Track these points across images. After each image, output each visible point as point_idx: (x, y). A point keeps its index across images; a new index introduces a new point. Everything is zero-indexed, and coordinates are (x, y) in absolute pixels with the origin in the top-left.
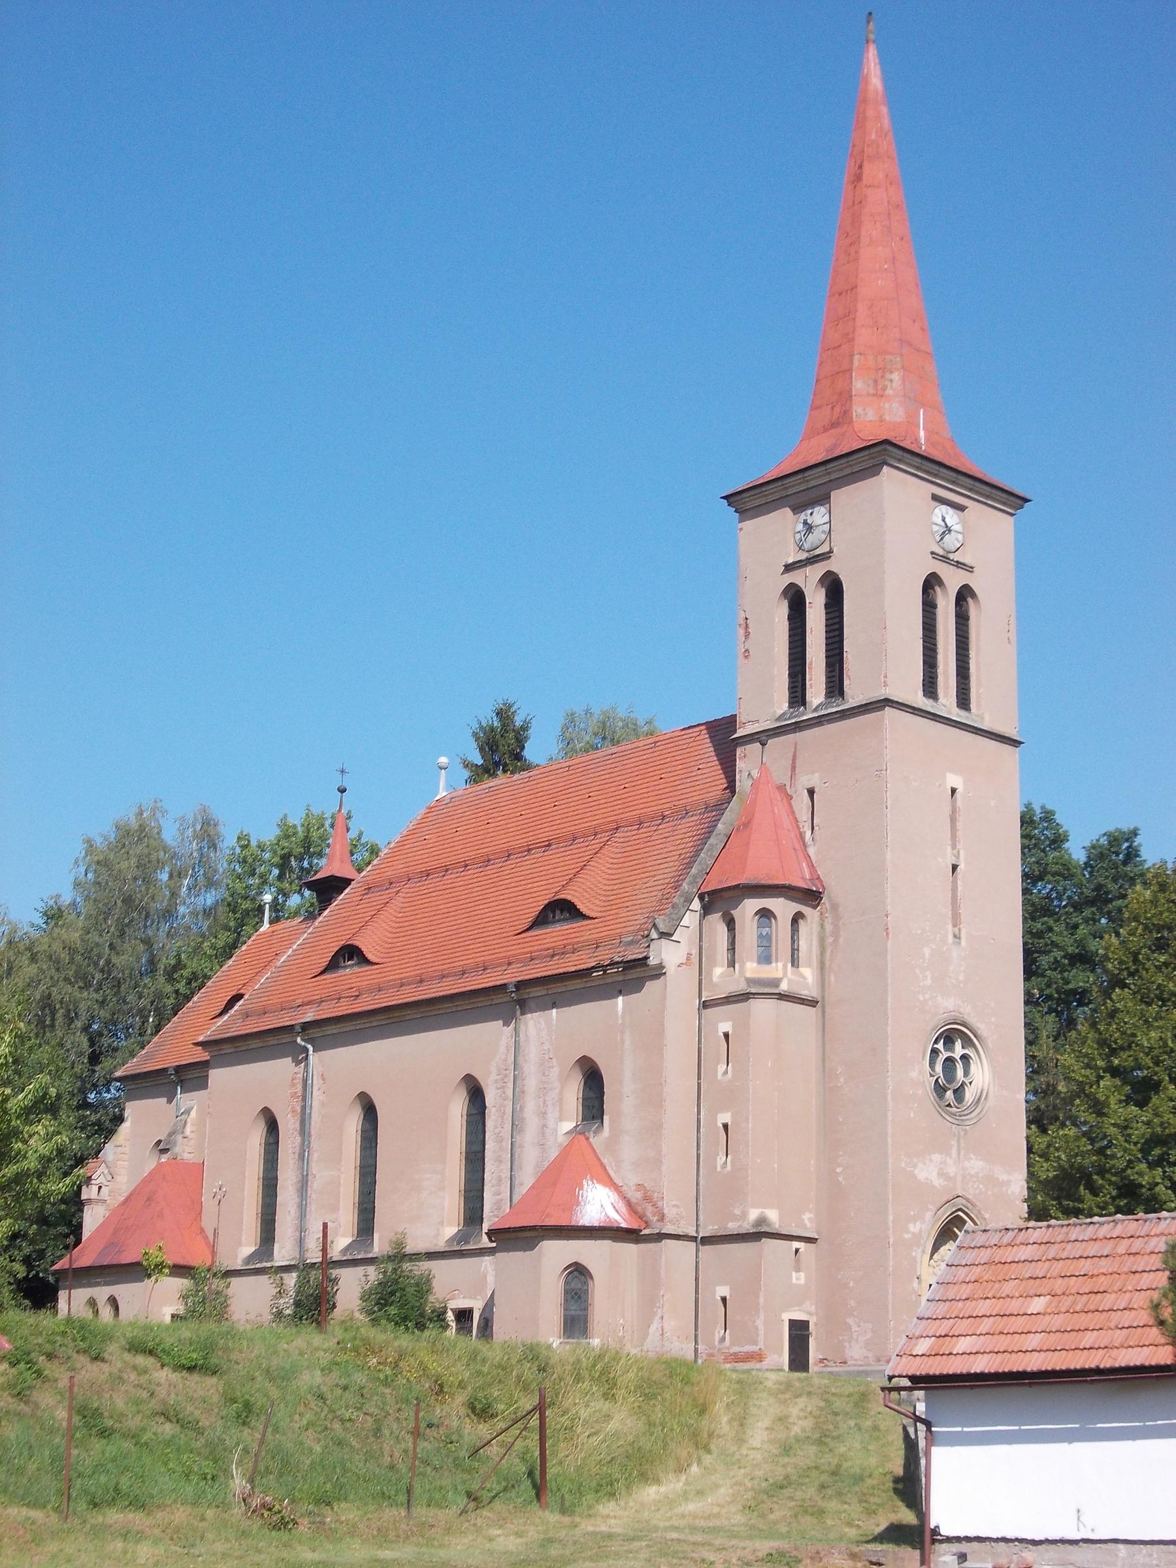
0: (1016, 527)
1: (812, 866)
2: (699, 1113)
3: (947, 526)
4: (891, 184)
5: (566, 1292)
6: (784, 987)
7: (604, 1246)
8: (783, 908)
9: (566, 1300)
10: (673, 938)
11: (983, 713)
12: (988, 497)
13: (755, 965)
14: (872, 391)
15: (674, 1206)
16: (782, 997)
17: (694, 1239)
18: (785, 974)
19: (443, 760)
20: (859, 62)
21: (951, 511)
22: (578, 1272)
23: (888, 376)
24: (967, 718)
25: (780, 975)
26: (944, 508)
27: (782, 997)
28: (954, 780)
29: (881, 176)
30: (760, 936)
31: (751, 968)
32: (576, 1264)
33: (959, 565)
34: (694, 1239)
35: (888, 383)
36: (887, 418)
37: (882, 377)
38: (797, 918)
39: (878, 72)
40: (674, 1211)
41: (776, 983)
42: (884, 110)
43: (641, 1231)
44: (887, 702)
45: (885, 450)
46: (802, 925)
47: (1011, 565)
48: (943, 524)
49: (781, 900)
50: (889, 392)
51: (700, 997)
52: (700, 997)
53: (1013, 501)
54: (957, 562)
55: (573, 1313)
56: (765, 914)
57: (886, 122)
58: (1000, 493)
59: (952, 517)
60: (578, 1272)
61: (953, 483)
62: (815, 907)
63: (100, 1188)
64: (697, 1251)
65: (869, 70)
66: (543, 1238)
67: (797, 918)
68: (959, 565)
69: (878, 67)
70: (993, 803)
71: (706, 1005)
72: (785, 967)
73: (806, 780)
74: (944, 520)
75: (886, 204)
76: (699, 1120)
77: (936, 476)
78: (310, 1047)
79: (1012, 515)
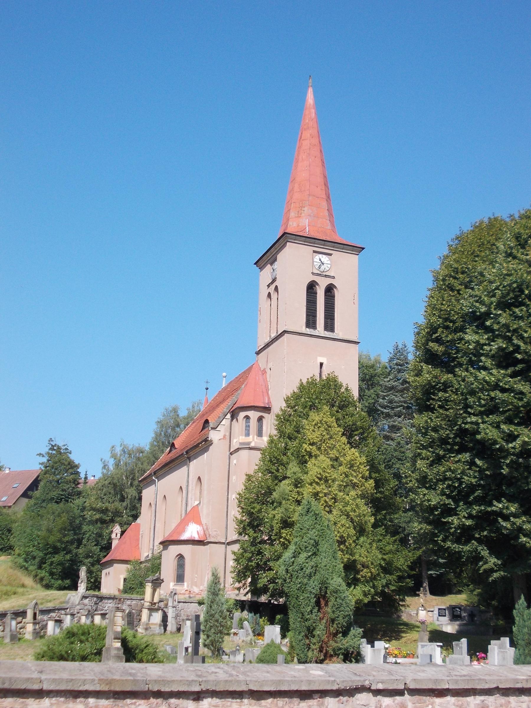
0: (359, 259)
1: (269, 398)
2: (228, 495)
3: (321, 262)
4: (312, 137)
5: (178, 565)
6: (253, 445)
7: (189, 547)
8: (254, 415)
9: (178, 568)
10: (217, 429)
11: (339, 332)
12: (343, 249)
13: (244, 437)
14: (296, 215)
15: (215, 531)
16: (251, 449)
17: (224, 543)
18: (253, 440)
19: (224, 374)
20: (306, 94)
21: (324, 256)
22: (181, 557)
23: (303, 209)
24: (333, 335)
25: (251, 440)
26: (320, 256)
27: (251, 449)
28: (320, 359)
29: (309, 135)
30: (246, 426)
31: (243, 439)
32: (180, 554)
33: (326, 276)
34: (224, 543)
35: (303, 212)
36: (300, 225)
37: (301, 210)
38: (260, 419)
39: (312, 97)
40: (215, 533)
41: (249, 443)
42: (313, 111)
43: (204, 541)
44: (285, 332)
45: (286, 236)
46: (265, 421)
47: (357, 274)
48: (320, 262)
49: (253, 411)
50: (303, 215)
51: (230, 450)
52: (230, 450)
53: (358, 250)
54: (325, 275)
55: (180, 573)
56: (247, 418)
57: (313, 115)
58: (348, 247)
59: (325, 258)
60: (181, 557)
61: (324, 245)
62: (269, 413)
63: (117, 534)
64: (226, 547)
65: (308, 98)
66: (169, 545)
67: (260, 419)
68: (326, 276)
69: (312, 95)
70: (343, 367)
71: (231, 454)
72: (253, 437)
73: (269, 367)
74: (320, 260)
75: (309, 145)
76: (228, 498)
77: (314, 243)
78: (157, 480)
79: (358, 255)
